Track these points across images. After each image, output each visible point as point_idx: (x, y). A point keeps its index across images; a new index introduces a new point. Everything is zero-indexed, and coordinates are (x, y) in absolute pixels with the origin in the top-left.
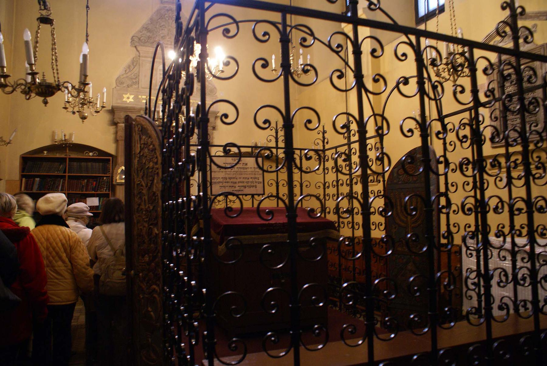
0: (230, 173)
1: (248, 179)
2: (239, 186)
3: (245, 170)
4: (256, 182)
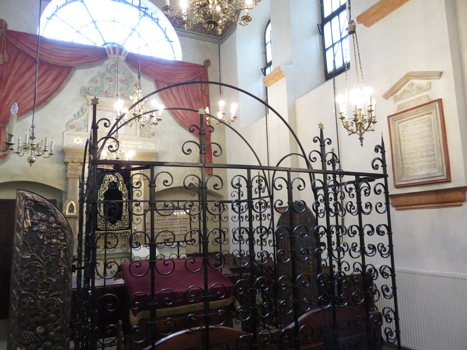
0: (162, 224)
1: (178, 228)
2: (169, 235)
3: (176, 221)
4: (184, 231)
